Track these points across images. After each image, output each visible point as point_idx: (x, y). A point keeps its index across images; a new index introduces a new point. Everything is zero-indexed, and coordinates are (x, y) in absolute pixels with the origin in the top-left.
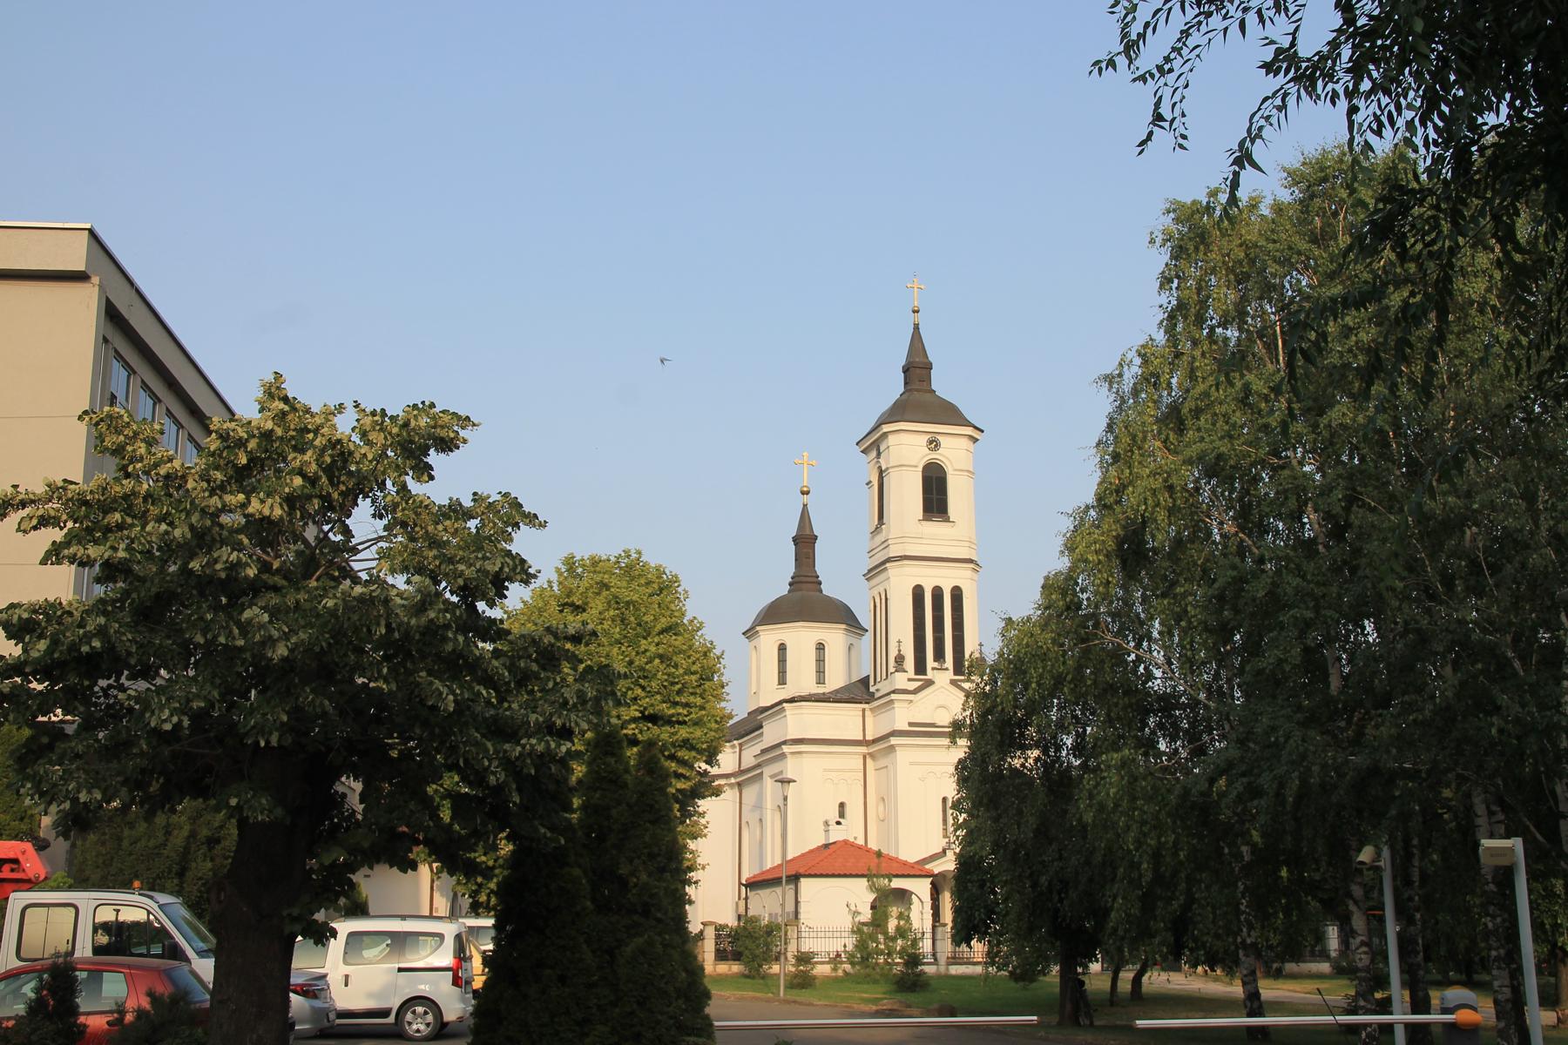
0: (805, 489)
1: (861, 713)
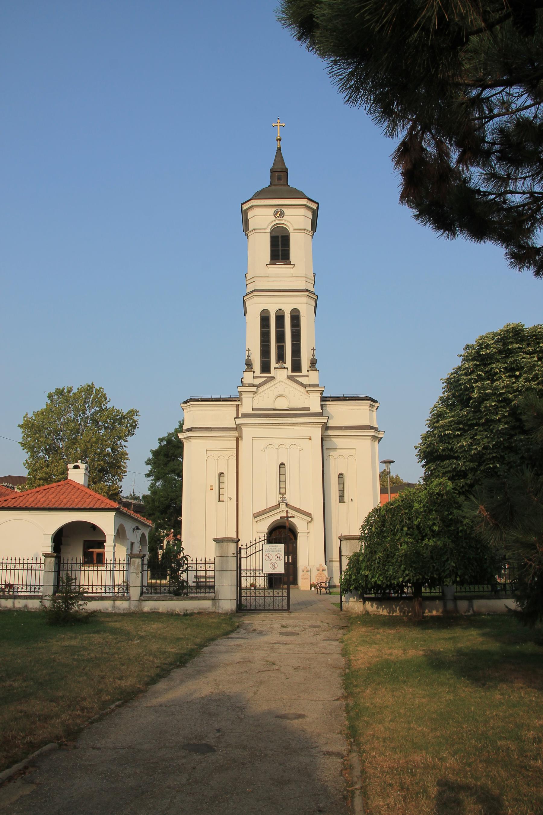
1: (236, 408)
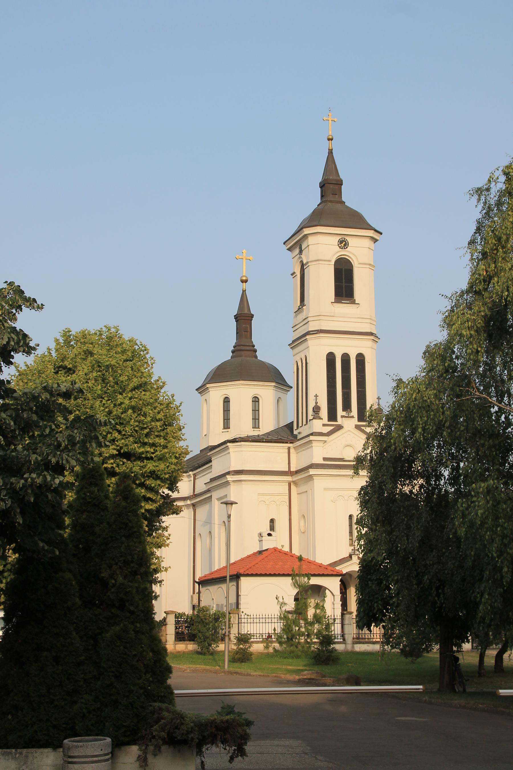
0: (244, 278)
